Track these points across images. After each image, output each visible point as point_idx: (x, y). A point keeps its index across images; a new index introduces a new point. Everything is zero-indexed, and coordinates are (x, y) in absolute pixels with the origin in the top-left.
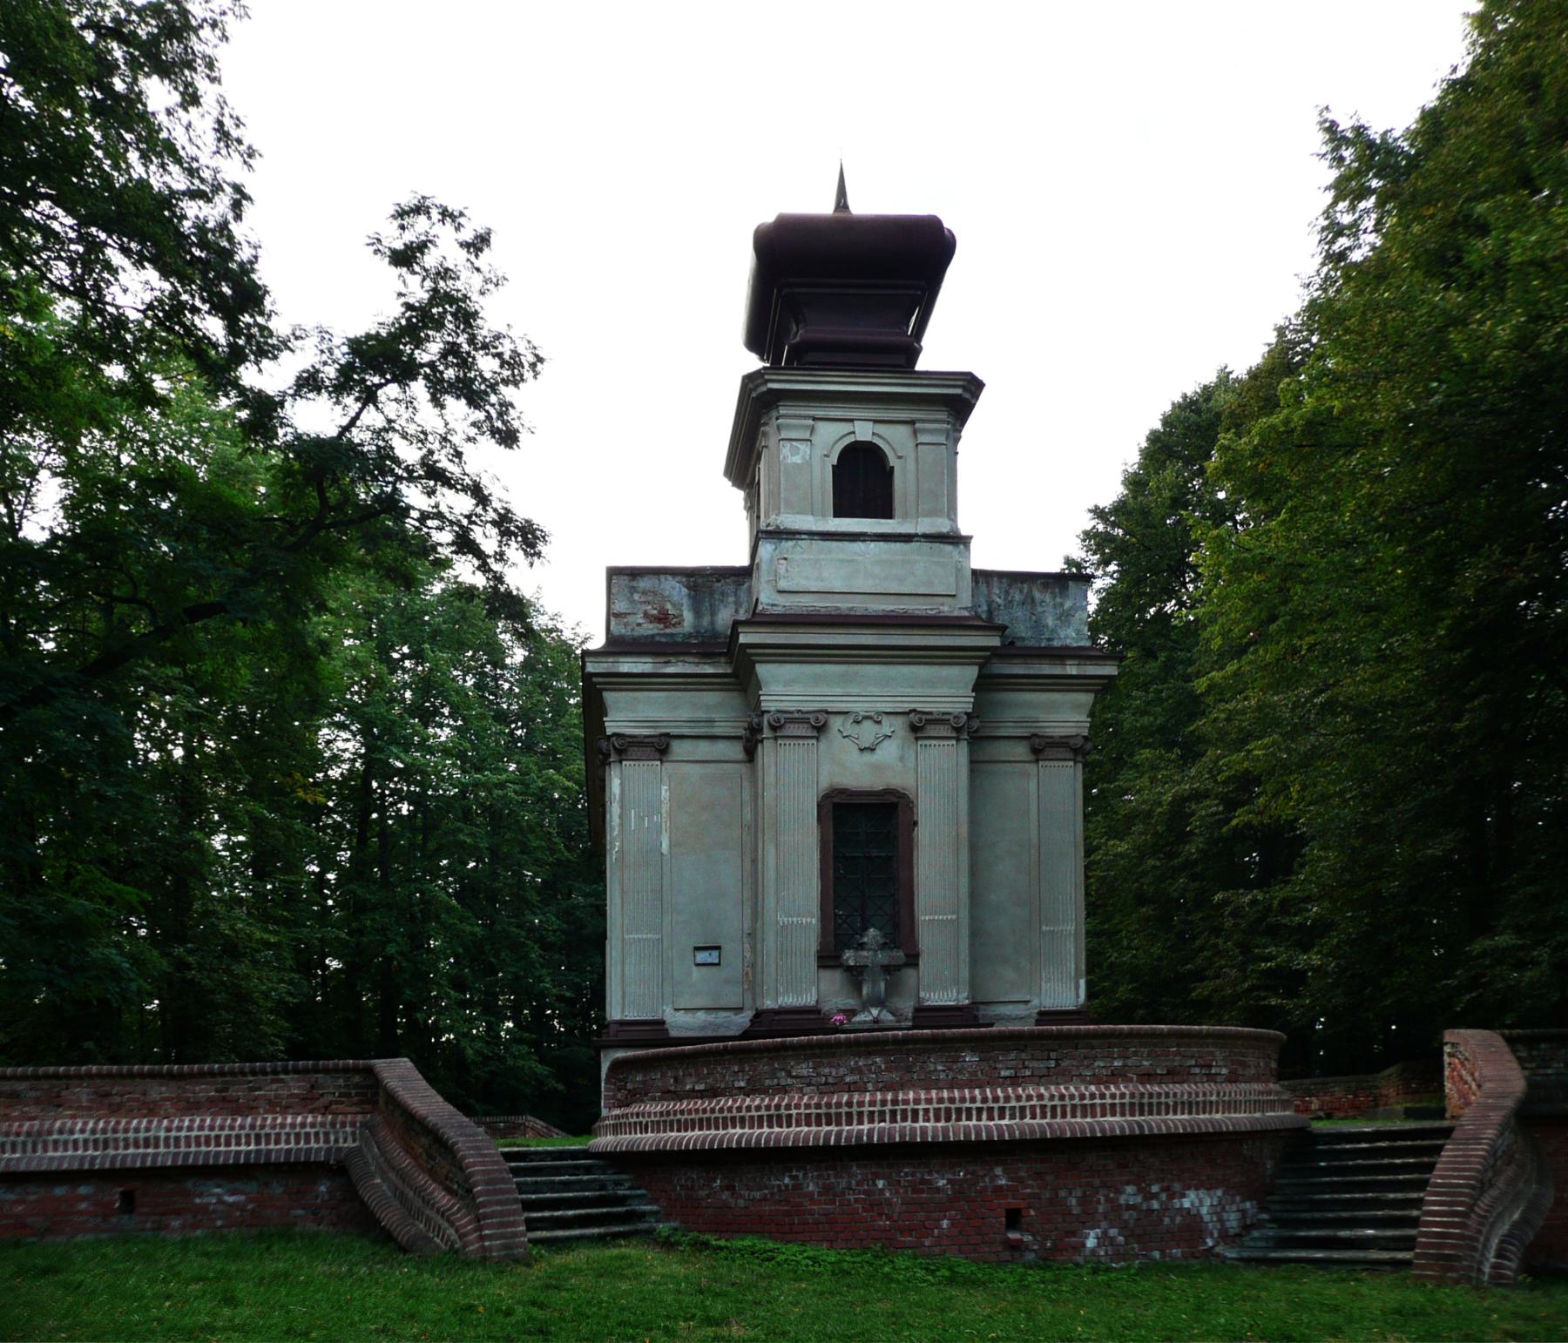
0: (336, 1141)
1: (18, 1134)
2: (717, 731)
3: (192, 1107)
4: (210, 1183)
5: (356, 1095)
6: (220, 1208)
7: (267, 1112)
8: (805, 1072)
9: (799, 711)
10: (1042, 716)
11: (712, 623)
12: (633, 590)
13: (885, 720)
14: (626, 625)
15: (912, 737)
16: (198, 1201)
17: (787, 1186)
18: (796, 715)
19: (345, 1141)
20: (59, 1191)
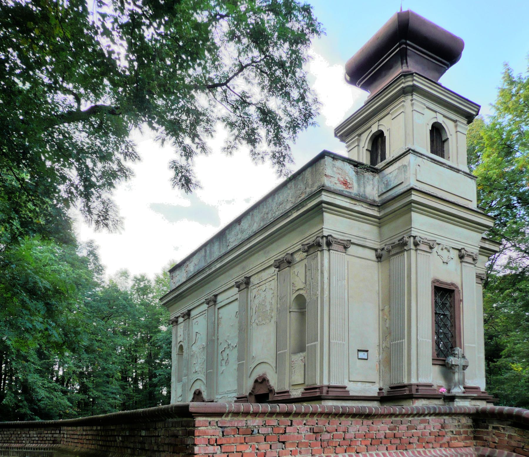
9: (426, 239)
11: (364, 191)
12: (334, 166)
13: (451, 250)
15: (459, 260)
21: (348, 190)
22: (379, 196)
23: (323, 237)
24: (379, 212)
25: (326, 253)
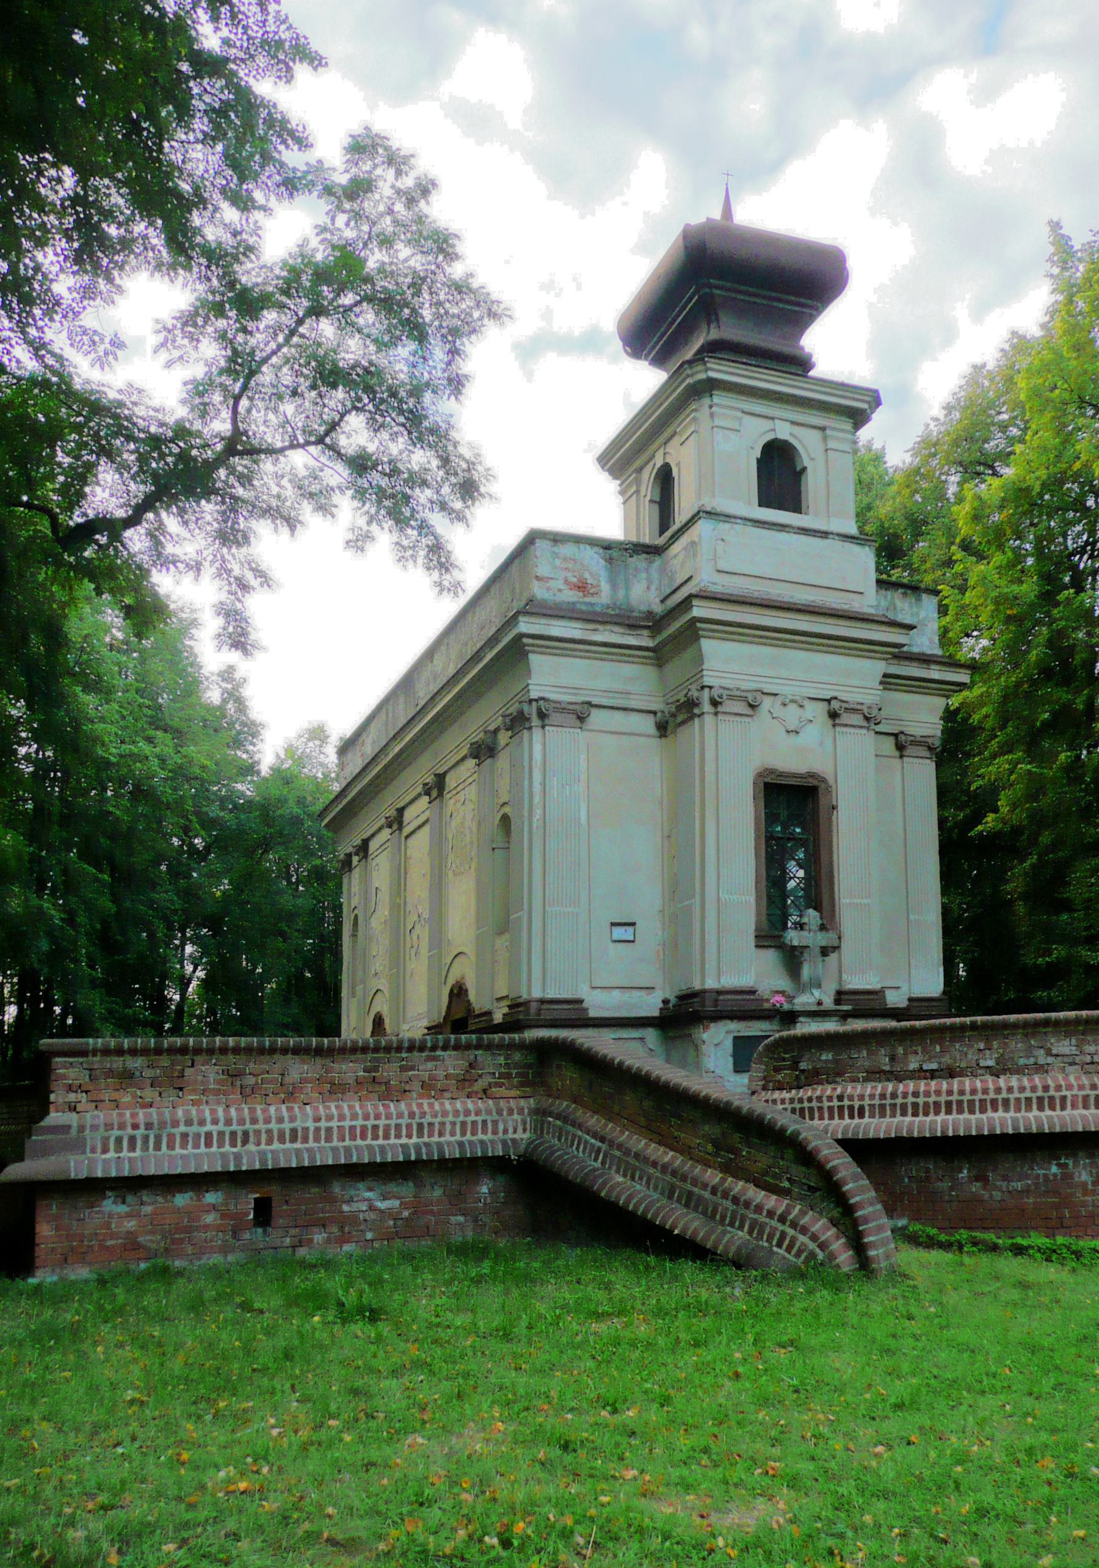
0: (506, 1131)
1: (135, 1127)
2: (633, 704)
3: (336, 1089)
4: (360, 1185)
5: (518, 1075)
6: (372, 1216)
7: (421, 1096)
8: (1066, 1050)
10: (904, 716)
11: (627, 596)
12: (556, 555)
13: (806, 703)
14: (548, 589)
16: (345, 1208)
17: (1055, 1175)
18: (738, 693)
19: (515, 1132)
20: (182, 1200)
21: (588, 599)
22: (662, 601)
23: (531, 701)
24: (653, 637)
25: (537, 734)
